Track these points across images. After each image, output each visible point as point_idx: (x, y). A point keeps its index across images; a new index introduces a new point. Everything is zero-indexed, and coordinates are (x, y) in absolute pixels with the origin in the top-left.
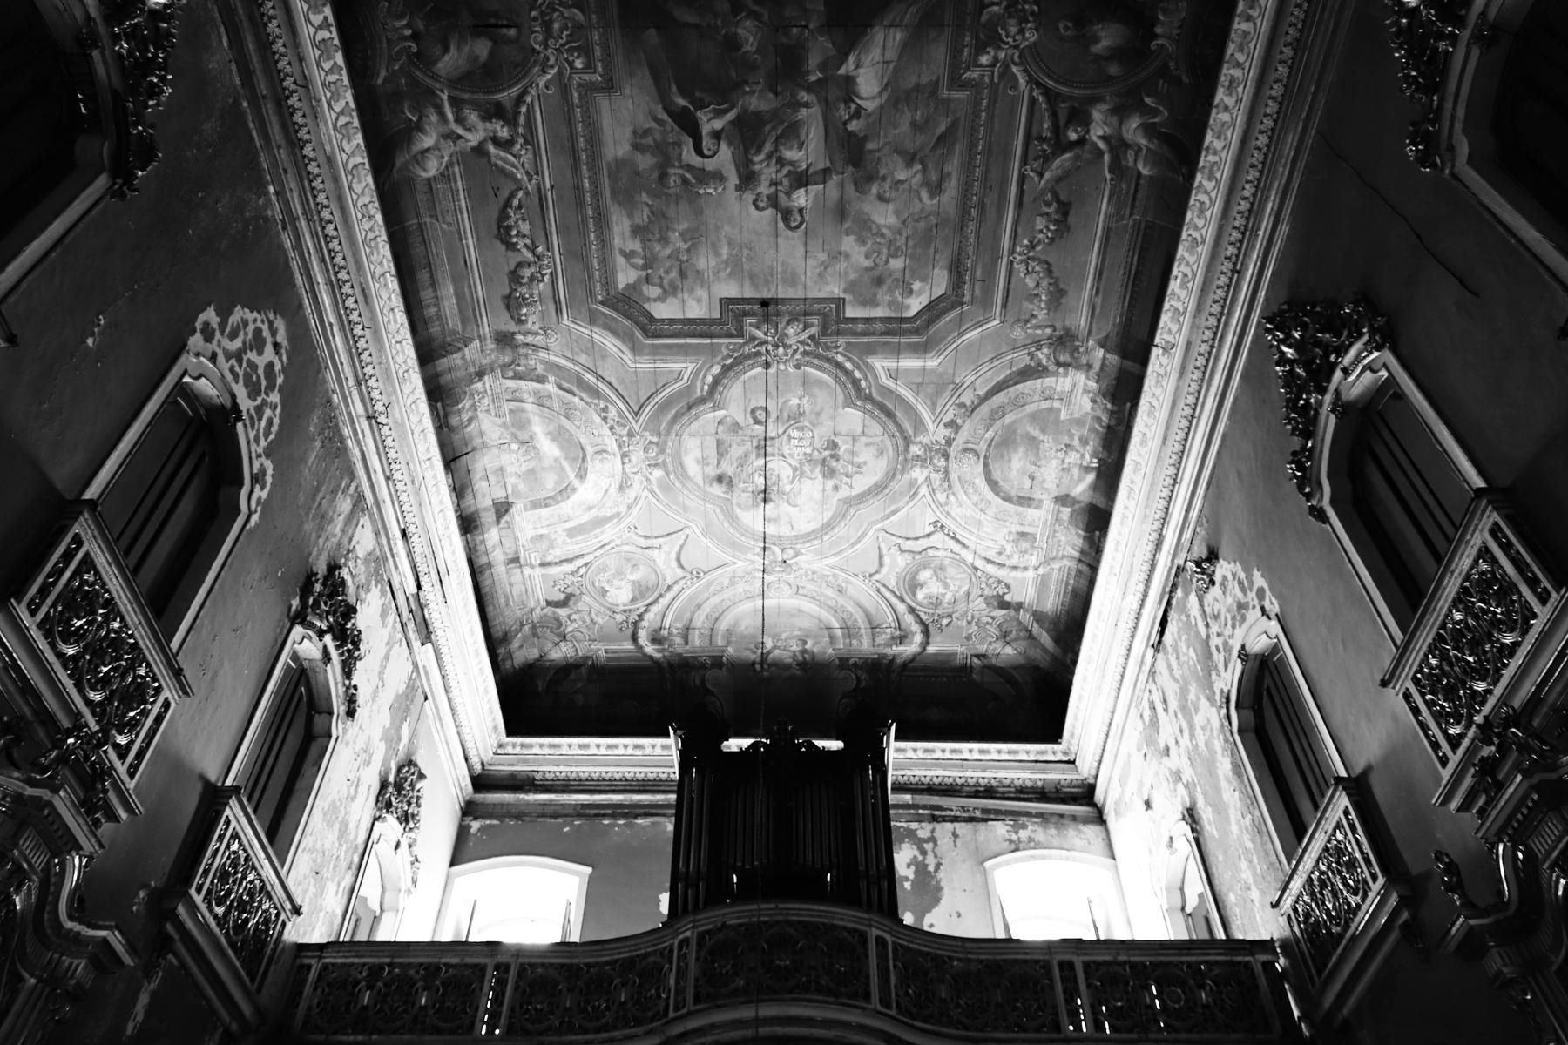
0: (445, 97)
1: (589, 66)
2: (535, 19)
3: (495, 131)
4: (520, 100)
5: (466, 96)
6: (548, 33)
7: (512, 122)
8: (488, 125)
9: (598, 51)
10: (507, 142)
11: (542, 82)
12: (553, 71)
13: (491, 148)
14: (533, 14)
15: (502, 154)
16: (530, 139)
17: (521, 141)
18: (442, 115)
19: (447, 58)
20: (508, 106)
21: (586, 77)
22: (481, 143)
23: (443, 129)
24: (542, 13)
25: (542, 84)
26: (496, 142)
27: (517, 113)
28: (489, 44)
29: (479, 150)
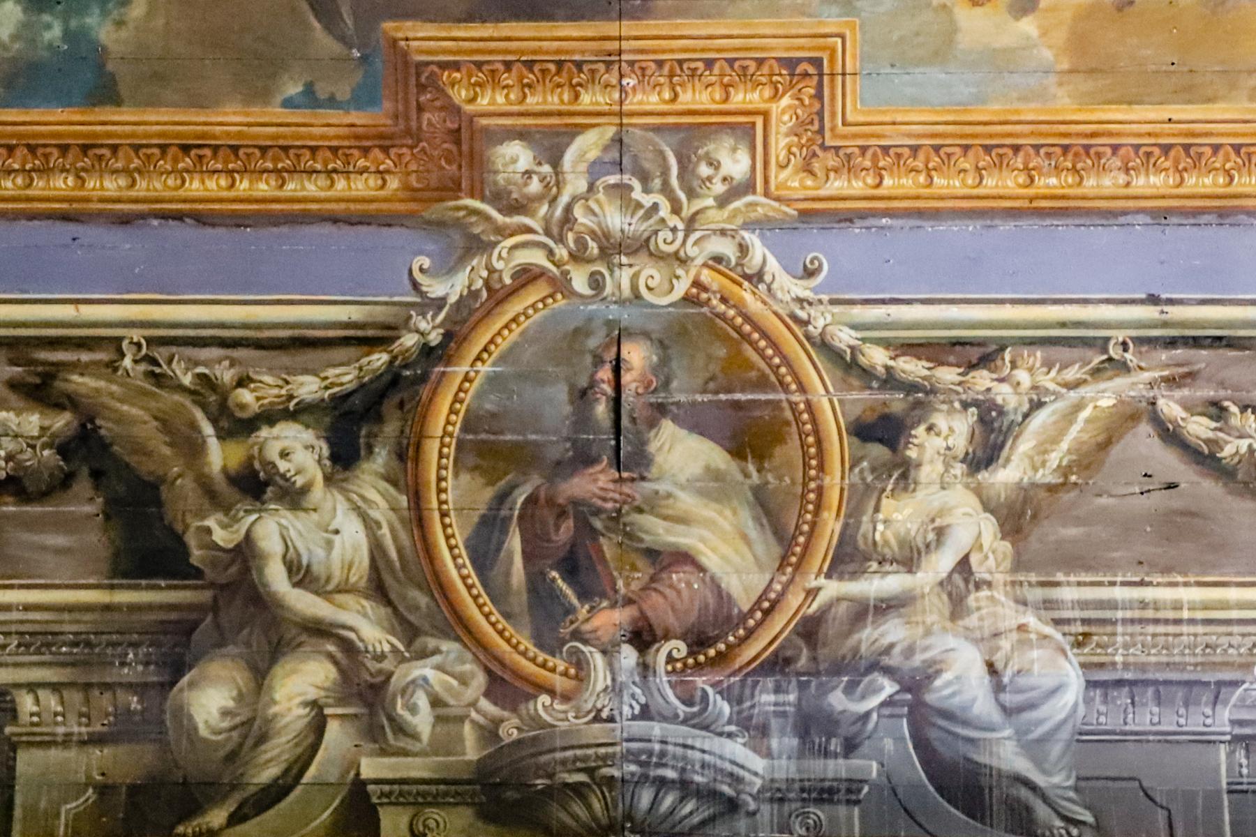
0: (832, 589)
1: (744, 129)
2: (596, 282)
3: (948, 456)
4: (849, 366)
5: (831, 525)
6: (641, 246)
7: (922, 398)
8: (929, 472)
9: (697, 97)
10: (983, 420)
11: (789, 287)
12: (758, 250)
13: (1007, 475)
14: (580, 283)
15: (1025, 445)
16: (980, 353)
17: (982, 380)
18: (885, 607)
19: (710, 560)
20: (861, 399)
21: (780, 144)
22: (987, 507)
23: (935, 609)
24: (578, 257)
25: (801, 289)
26: (985, 455)
27: (890, 380)
28: (668, 427)
29: (1016, 516)
